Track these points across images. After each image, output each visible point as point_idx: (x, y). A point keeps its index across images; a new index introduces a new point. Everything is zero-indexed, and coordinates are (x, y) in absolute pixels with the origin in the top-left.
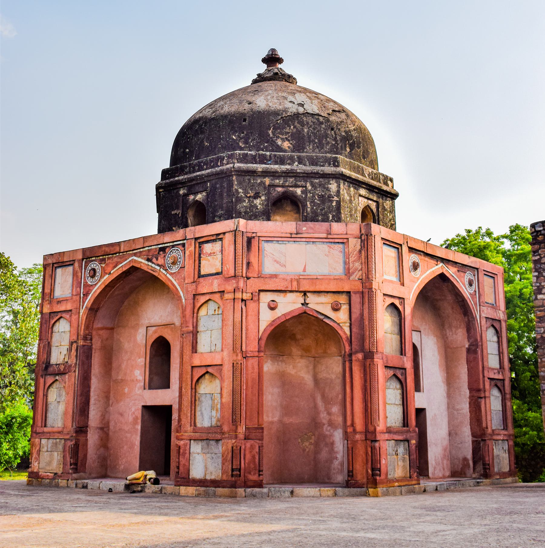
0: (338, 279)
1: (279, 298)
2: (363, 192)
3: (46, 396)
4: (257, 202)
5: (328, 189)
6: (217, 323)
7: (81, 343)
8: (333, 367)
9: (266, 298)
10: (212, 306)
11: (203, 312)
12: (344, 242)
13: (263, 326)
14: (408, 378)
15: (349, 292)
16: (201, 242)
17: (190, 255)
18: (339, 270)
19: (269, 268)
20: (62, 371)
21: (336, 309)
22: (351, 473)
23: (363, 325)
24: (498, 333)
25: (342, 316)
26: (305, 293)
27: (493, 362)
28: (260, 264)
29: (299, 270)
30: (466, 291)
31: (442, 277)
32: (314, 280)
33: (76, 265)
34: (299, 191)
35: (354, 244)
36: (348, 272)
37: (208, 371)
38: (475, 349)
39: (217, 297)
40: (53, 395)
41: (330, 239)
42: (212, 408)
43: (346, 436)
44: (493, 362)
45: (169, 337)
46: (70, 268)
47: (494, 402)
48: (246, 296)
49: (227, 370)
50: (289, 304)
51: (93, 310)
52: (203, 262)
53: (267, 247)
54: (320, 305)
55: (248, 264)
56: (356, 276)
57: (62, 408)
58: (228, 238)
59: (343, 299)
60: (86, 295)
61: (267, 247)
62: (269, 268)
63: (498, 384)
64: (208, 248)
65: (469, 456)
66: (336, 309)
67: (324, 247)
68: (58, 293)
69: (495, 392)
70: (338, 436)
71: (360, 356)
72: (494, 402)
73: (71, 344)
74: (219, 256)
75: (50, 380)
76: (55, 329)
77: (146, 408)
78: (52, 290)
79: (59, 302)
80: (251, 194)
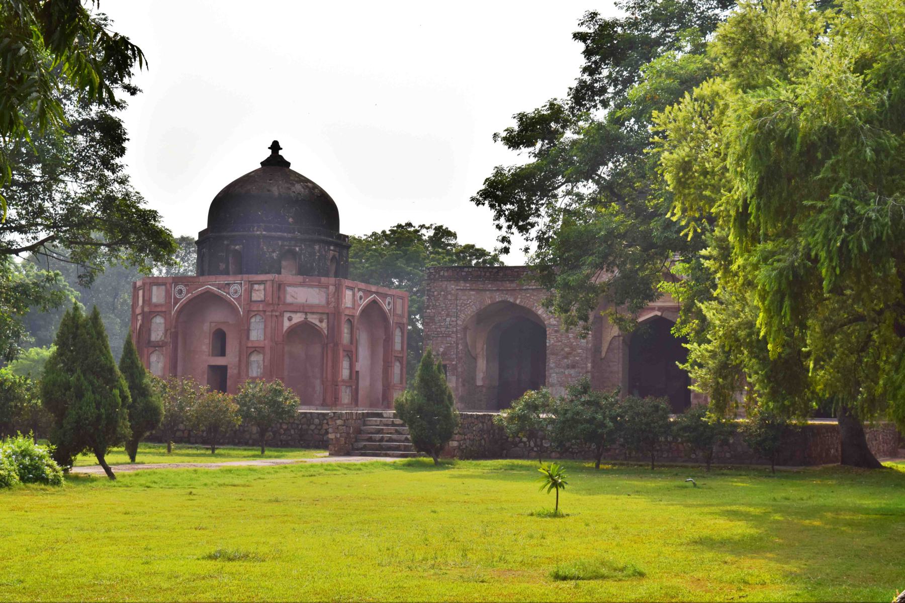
0: (323, 306)
1: (293, 315)
2: (332, 248)
3: (149, 358)
4: (274, 255)
5: (314, 249)
6: (262, 326)
7: (173, 330)
8: (316, 350)
9: (287, 315)
10: (258, 318)
11: (253, 320)
12: (327, 287)
13: (285, 328)
14: (352, 356)
15: (328, 314)
16: (252, 283)
17: (245, 290)
18: (323, 302)
19: (289, 299)
20: (158, 346)
21: (321, 321)
22: (324, 400)
23: (334, 329)
24: (402, 331)
25: (324, 325)
26: (306, 313)
27: (398, 346)
28: (285, 297)
29: (304, 301)
30: (386, 308)
31: (374, 302)
32: (311, 306)
33: (168, 285)
34: (297, 249)
35: (332, 289)
36: (328, 303)
37: (257, 350)
38: (389, 340)
39: (262, 313)
40: (153, 358)
41: (320, 286)
42: (258, 367)
43: (323, 383)
44: (398, 346)
45: (225, 329)
46: (164, 287)
47: (397, 369)
48: (277, 314)
49: (268, 351)
50: (298, 318)
51: (180, 312)
52: (253, 294)
53: (289, 289)
54: (313, 319)
55: (279, 298)
56: (333, 304)
57: (160, 365)
58: (269, 284)
59: (325, 317)
60: (175, 304)
61: (289, 289)
62: (289, 299)
63: (400, 359)
64: (256, 287)
65: (380, 397)
66: (321, 321)
67: (317, 290)
68: (154, 300)
69: (398, 364)
70: (318, 382)
71: (332, 345)
72: (397, 369)
73: (166, 331)
74: (263, 292)
75: (151, 349)
76: (154, 320)
77: (213, 368)
78: (150, 298)
79: (156, 306)
80: (271, 250)
